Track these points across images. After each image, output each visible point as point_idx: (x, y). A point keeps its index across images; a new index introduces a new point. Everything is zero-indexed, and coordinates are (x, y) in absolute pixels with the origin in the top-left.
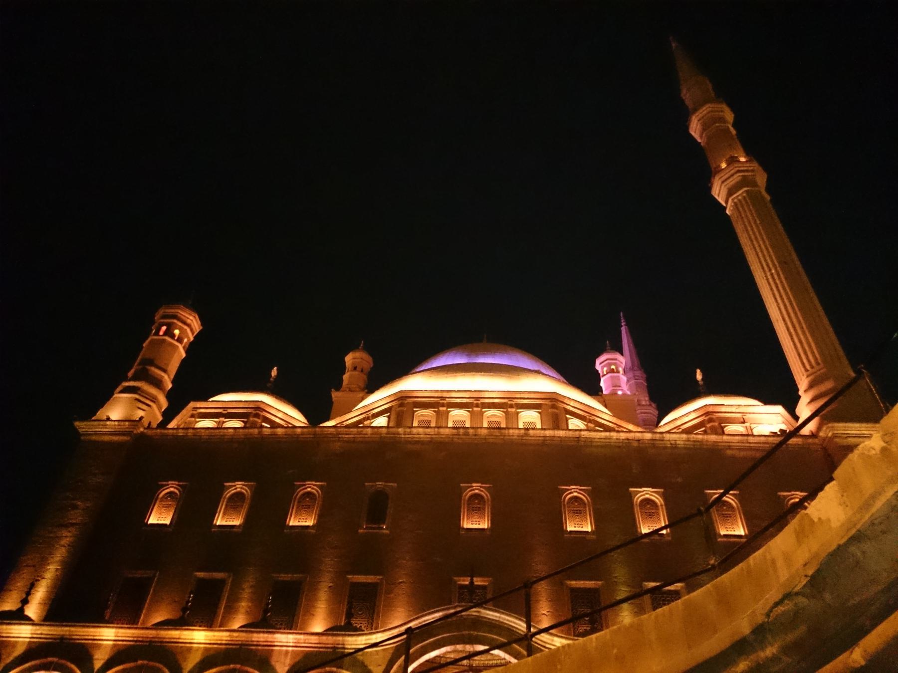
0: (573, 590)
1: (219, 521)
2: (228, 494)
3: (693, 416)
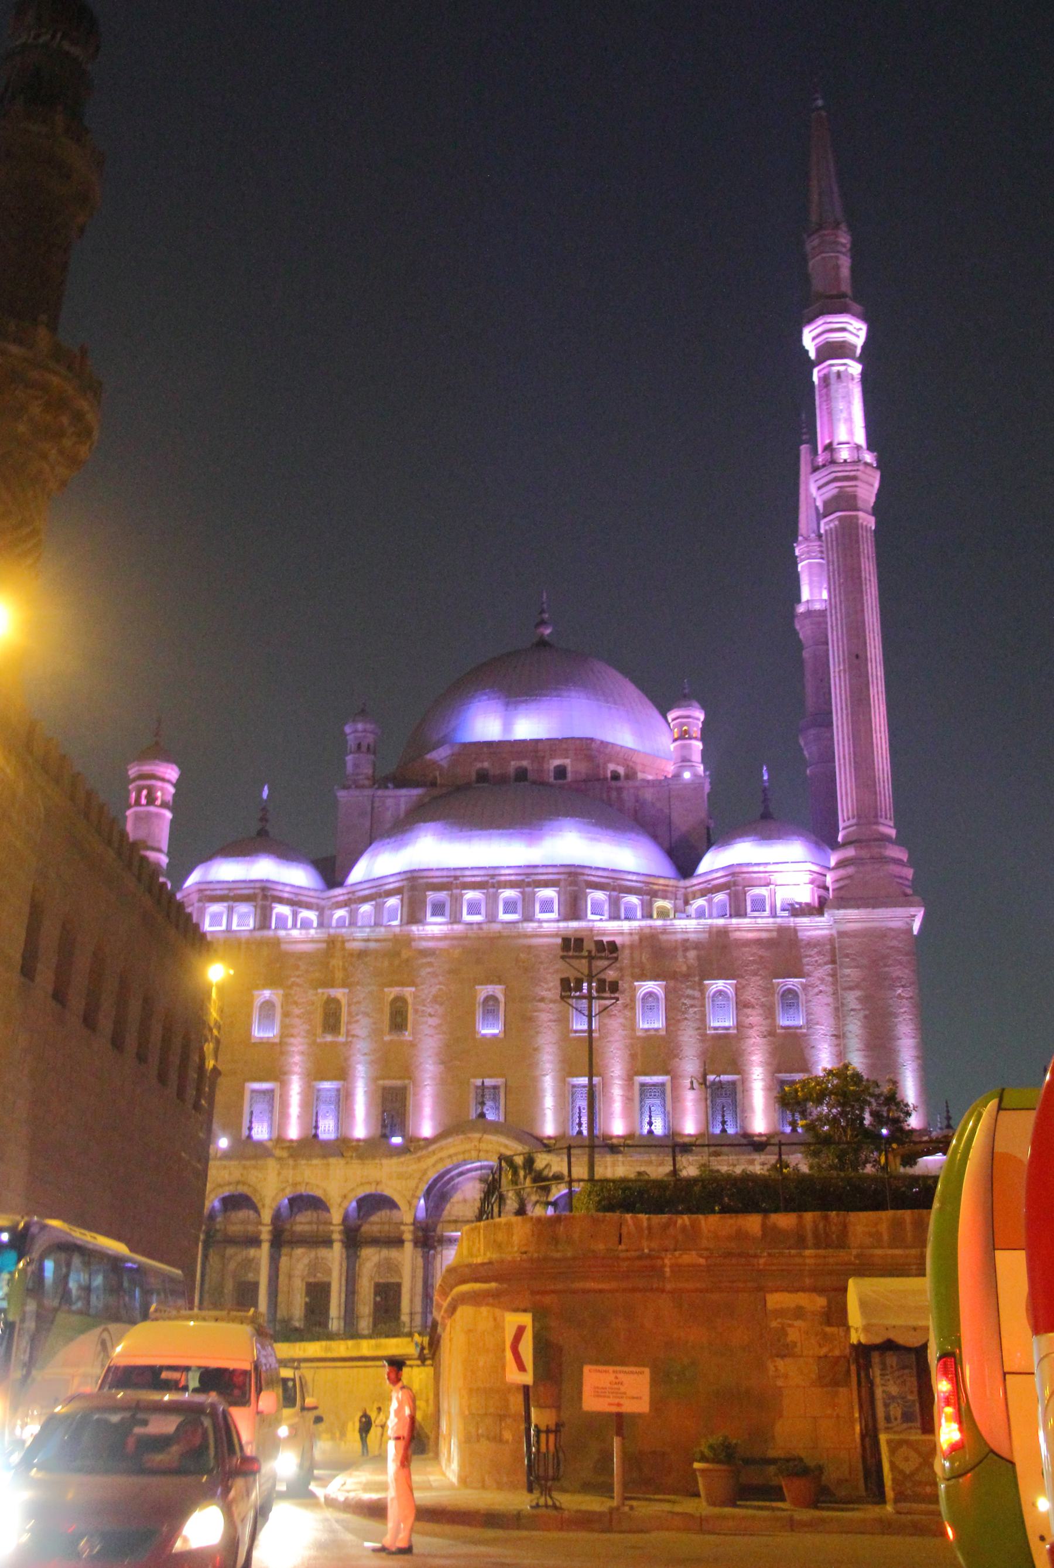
2: (257, 1003)
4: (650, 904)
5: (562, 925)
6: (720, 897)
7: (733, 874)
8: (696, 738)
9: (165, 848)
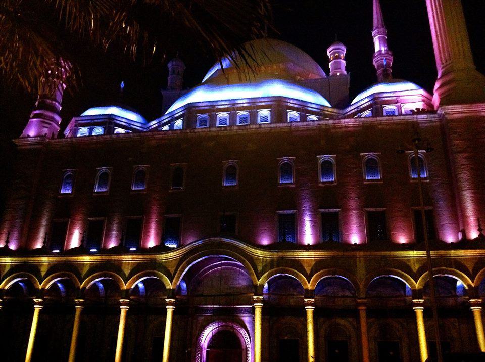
0: (281, 215)
2: (99, 174)
3: (367, 100)
5: (273, 126)
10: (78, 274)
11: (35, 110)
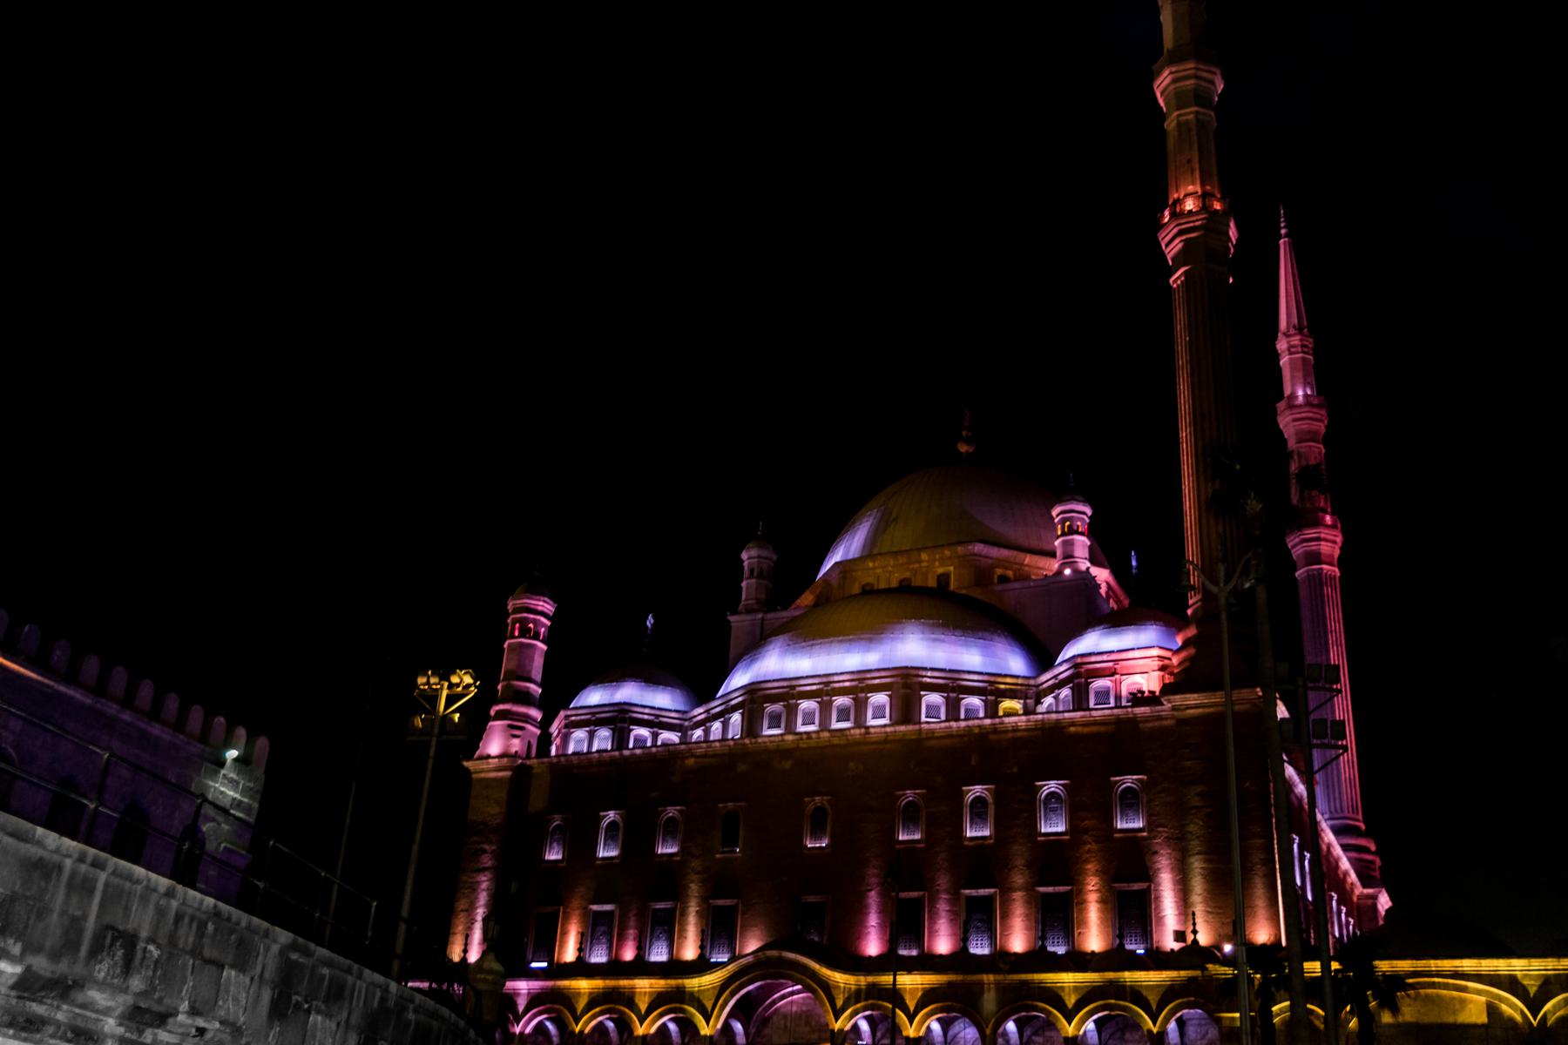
1: (602, 853)
2: (604, 824)
4: (997, 703)
6: (1065, 692)
7: (1076, 666)
8: (1082, 534)
9: (539, 678)
10: (573, 1011)
11: (498, 703)
